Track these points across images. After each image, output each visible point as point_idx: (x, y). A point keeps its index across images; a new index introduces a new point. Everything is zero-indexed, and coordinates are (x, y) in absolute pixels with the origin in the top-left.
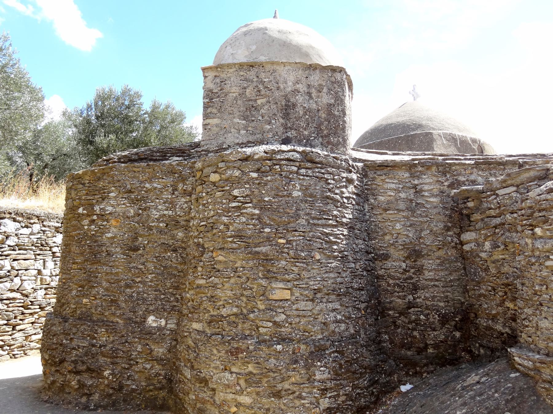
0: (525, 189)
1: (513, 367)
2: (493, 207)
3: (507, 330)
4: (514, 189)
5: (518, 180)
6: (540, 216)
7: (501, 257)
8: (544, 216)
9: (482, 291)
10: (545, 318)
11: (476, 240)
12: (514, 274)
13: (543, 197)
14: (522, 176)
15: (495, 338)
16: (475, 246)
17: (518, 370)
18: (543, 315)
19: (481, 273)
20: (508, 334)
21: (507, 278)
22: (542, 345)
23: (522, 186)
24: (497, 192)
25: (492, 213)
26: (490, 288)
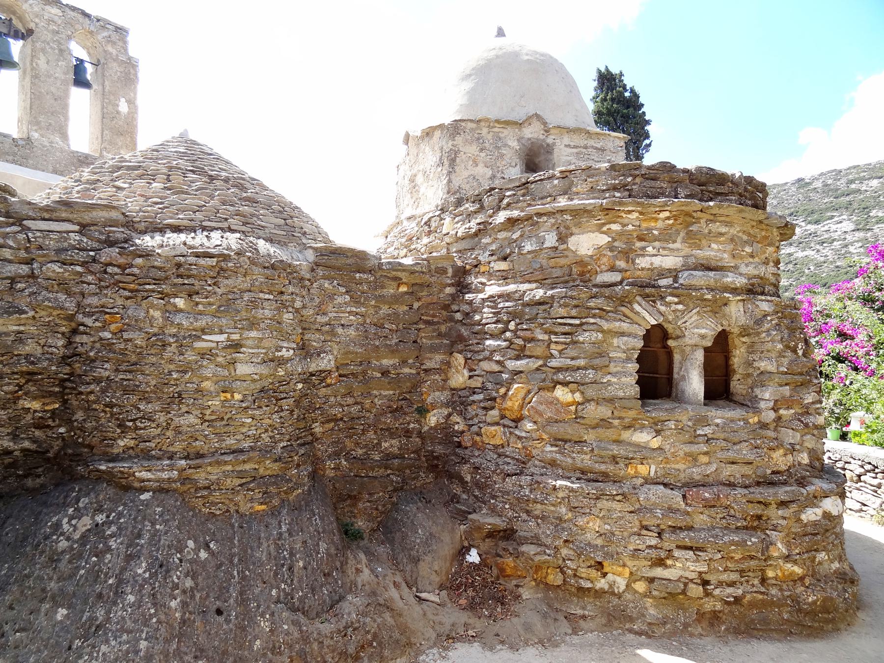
0: (101, 233)
1: (126, 487)
2: (11, 243)
4: (77, 228)
5: (87, 217)
6: (184, 284)
7: (15, 328)
8: (193, 285)
10: (187, 412)
12: (47, 356)
13: (192, 259)
14: (94, 213)
17: (143, 490)
18: (184, 409)
20: (23, 450)
21: (33, 363)
22: (178, 447)
23: (96, 227)
24: (25, 222)
25: (7, 253)
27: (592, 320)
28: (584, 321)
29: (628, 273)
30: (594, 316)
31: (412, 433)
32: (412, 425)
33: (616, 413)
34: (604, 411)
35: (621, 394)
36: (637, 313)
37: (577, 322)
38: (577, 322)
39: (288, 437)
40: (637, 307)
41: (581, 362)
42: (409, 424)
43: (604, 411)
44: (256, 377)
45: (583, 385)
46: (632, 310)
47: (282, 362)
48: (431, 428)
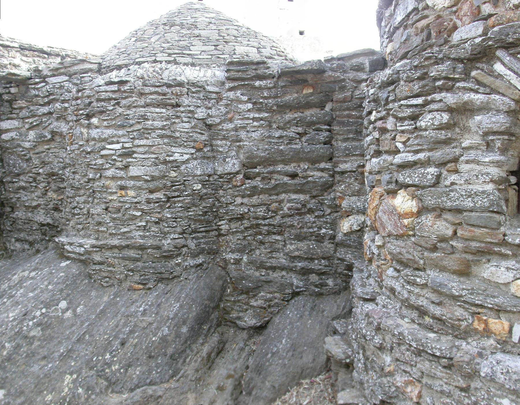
1: (63, 255)
3: (49, 221)
9: (23, 184)
11: (17, 129)
15: (35, 230)
16: (17, 135)
19: (21, 164)
26: (31, 180)
27: (437, 96)
28: (429, 98)
29: (493, 19)
30: (441, 89)
31: (323, 237)
32: (323, 231)
33: (460, 233)
34: (443, 227)
35: (468, 203)
36: (499, 76)
37: (419, 101)
38: (419, 101)
39: (179, 230)
40: (498, 67)
41: (421, 156)
42: (320, 228)
43: (443, 227)
44: (146, 178)
45: (423, 187)
46: (491, 73)
47: (176, 165)
48: (345, 235)
